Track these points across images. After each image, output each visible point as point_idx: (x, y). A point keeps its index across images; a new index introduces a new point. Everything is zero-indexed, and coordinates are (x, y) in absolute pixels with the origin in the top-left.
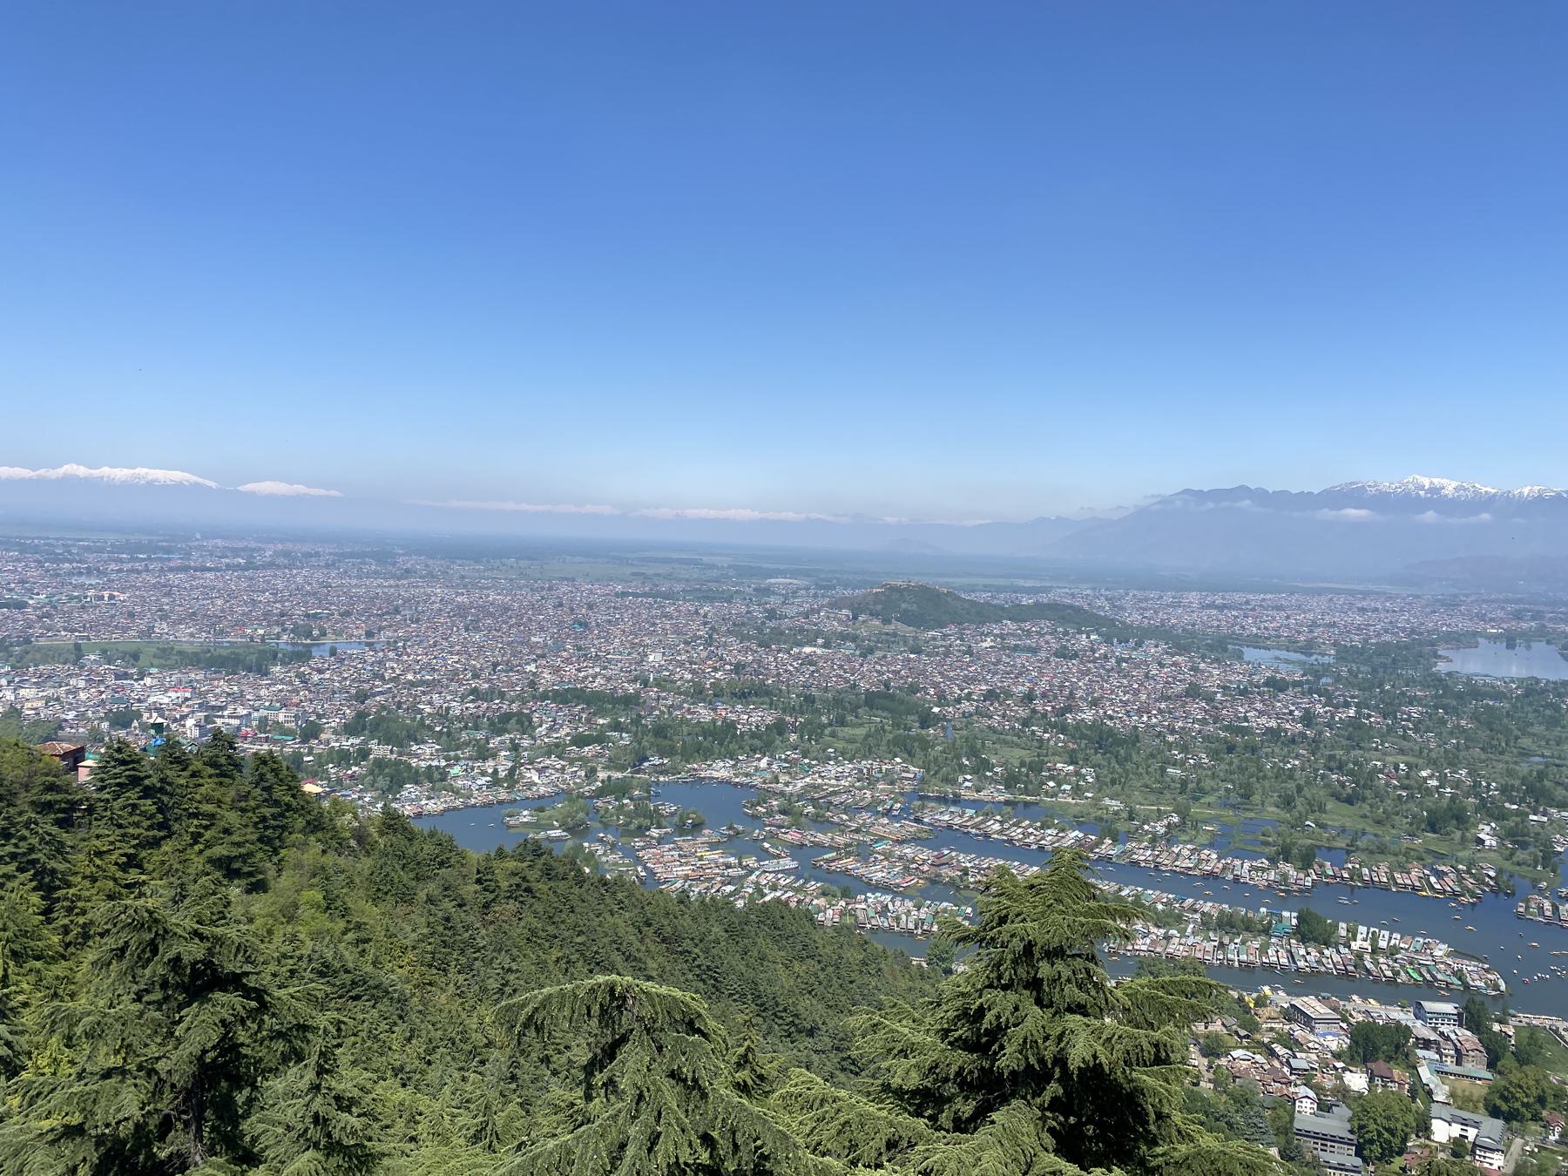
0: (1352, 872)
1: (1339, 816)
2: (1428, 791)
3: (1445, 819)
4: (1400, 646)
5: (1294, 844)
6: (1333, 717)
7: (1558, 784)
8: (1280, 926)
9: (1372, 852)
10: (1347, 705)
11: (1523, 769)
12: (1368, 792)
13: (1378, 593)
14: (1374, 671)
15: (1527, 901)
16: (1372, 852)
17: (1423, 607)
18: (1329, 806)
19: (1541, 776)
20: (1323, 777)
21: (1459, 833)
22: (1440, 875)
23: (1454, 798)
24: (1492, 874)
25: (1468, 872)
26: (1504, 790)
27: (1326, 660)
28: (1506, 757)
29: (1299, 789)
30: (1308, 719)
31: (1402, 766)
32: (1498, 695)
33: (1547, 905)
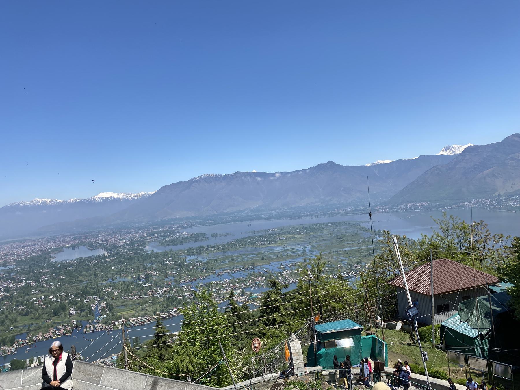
0: (29, 340)
1: (22, 321)
2: (53, 303)
3: (60, 310)
4: (38, 257)
5: (6, 338)
6: (17, 287)
7: (91, 288)
8: (4, 370)
9: (36, 330)
10: (22, 281)
11: (81, 287)
12: (32, 310)
13: (29, 240)
14: (30, 267)
15: (86, 327)
16: (36, 330)
17: (45, 242)
18: (19, 319)
19: (86, 287)
20: (15, 309)
21: (64, 313)
22: (59, 329)
23: (61, 302)
24: (75, 323)
25: (68, 325)
26: (76, 295)
27: (12, 267)
28: (76, 285)
29: (6, 317)
30: (7, 290)
31: (43, 297)
32: (71, 265)
33: (92, 326)
